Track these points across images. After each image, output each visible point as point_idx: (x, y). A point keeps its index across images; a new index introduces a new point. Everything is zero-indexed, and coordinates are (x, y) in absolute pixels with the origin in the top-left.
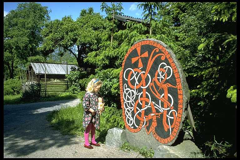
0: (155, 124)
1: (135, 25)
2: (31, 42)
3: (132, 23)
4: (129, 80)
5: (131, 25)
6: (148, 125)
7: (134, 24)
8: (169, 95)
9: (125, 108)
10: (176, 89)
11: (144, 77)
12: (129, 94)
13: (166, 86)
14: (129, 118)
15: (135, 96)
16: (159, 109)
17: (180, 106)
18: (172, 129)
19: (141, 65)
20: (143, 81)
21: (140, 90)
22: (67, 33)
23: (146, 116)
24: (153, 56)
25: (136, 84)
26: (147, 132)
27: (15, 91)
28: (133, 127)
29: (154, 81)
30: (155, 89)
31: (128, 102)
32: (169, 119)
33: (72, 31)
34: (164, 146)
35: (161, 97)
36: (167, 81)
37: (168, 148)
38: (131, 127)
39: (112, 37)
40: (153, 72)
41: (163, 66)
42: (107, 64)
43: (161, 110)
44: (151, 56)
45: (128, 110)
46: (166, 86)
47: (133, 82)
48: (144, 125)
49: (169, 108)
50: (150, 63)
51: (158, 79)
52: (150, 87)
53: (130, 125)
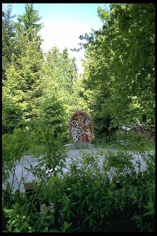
0: (85, 138)
12: (75, 130)
29: (85, 126)
40: (84, 122)
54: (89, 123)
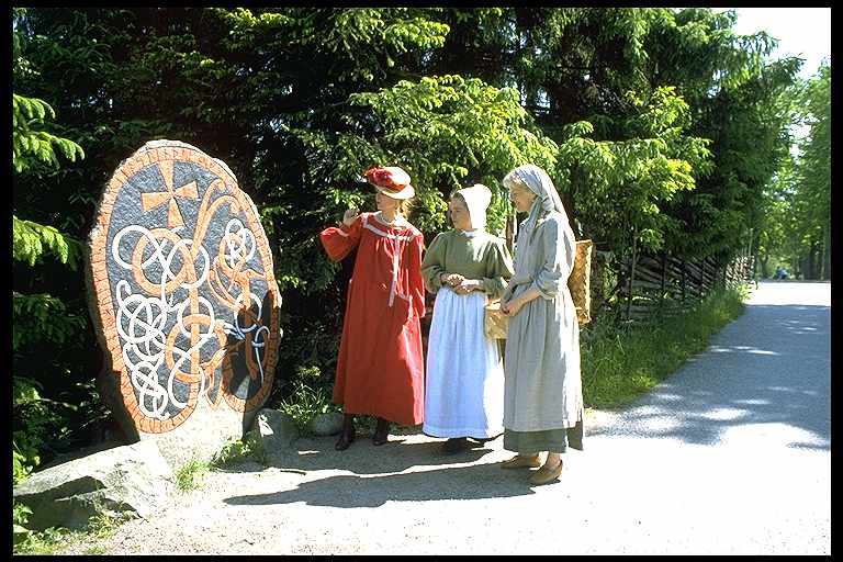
4: (137, 267)
6: (211, 385)
10: (265, 281)
12: (142, 317)
15: (163, 316)
19: (175, 218)
20: (189, 267)
25: (164, 278)
28: (168, 415)
31: (140, 340)
40: (212, 247)
41: (234, 230)
47: (153, 274)
50: (204, 220)
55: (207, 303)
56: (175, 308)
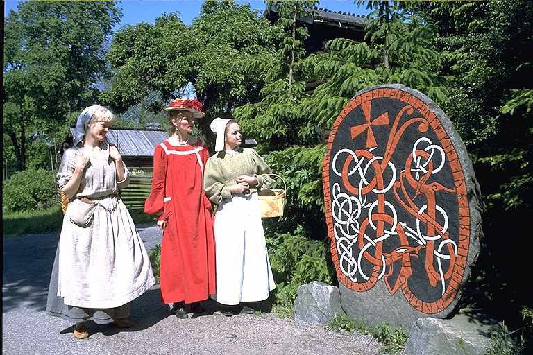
0: (406, 272)
1: (350, 47)
2: (70, 75)
3: (343, 41)
4: (345, 175)
5: (341, 45)
6: (390, 274)
7: (347, 46)
8: (438, 208)
9: (337, 238)
11: (379, 170)
12: (346, 207)
13: (430, 189)
14: (346, 258)
16: (415, 238)
17: (463, 232)
18: (447, 282)
19: (371, 142)
21: (371, 197)
22: (173, 57)
23: (387, 255)
24: (401, 123)
26: (390, 289)
27: (38, 200)
28: (356, 280)
29: (404, 178)
30: (406, 195)
31: (344, 223)
32: (439, 260)
33: (184, 53)
34: (430, 319)
35: (420, 212)
36: (433, 178)
37: (440, 323)
38: (352, 279)
39: (291, 70)
40: (401, 158)
41: (423, 146)
42: (282, 135)
43: (421, 242)
44: (396, 123)
45: (343, 242)
46: (430, 189)
47: (355, 179)
48: (383, 274)
49: (439, 237)
50: (394, 139)
51: (413, 174)
52: (395, 190)
53: (350, 275)
54: (437, 160)
55: (392, 207)
56: (368, 206)
